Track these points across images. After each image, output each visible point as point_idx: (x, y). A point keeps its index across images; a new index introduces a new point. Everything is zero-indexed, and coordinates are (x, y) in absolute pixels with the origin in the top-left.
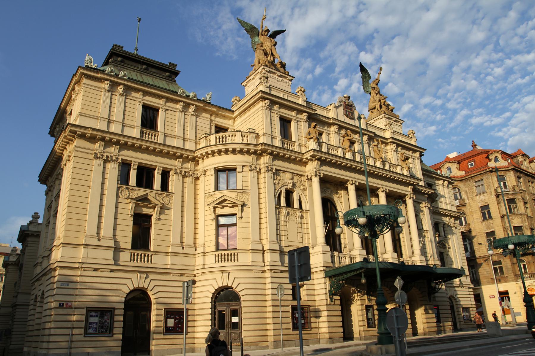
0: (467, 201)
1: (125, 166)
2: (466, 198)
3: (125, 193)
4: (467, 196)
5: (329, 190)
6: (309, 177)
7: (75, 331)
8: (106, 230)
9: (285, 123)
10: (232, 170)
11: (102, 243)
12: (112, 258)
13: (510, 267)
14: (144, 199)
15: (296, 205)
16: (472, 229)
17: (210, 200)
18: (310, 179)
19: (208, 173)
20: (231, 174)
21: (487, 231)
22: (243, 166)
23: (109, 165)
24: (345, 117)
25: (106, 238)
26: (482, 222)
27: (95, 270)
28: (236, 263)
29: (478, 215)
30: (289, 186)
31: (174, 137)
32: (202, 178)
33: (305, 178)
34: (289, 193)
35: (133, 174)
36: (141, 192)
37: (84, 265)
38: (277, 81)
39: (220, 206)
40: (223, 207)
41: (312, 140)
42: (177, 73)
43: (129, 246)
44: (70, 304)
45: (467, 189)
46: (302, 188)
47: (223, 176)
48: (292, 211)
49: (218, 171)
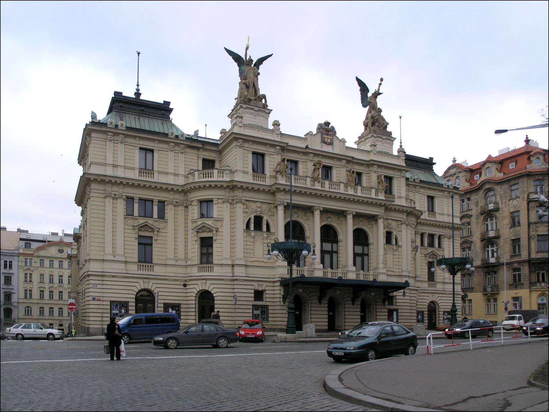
0: (500, 206)
1: (130, 200)
2: (500, 202)
3: (130, 222)
4: (501, 200)
5: (296, 215)
6: (276, 205)
7: (105, 315)
8: (120, 250)
9: (259, 157)
10: (209, 202)
11: (117, 258)
12: (124, 268)
13: (528, 275)
14: (145, 227)
15: (264, 228)
16: (501, 235)
17: (195, 225)
18: (276, 207)
19: (193, 204)
20: (211, 203)
21: (513, 238)
22: (218, 199)
23: (119, 201)
24: (323, 144)
25: (119, 255)
26: (510, 228)
27: (113, 276)
28: (212, 274)
29: (507, 221)
30: (258, 214)
31: (167, 173)
32: (190, 207)
33: (272, 206)
34: (258, 220)
35: (136, 206)
36: (142, 221)
37: (105, 274)
38: (255, 116)
39: (200, 231)
40: (203, 231)
41: (279, 173)
42: (171, 110)
43: (136, 260)
44: (99, 298)
45: (502, 192)
46: (270, 213)
47: (205, 205)
48: (259, 233)
49: (201, 202)
